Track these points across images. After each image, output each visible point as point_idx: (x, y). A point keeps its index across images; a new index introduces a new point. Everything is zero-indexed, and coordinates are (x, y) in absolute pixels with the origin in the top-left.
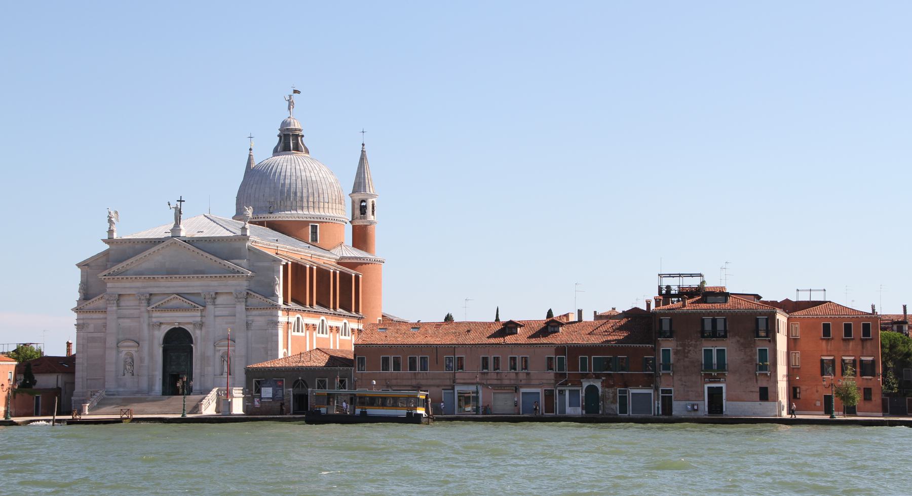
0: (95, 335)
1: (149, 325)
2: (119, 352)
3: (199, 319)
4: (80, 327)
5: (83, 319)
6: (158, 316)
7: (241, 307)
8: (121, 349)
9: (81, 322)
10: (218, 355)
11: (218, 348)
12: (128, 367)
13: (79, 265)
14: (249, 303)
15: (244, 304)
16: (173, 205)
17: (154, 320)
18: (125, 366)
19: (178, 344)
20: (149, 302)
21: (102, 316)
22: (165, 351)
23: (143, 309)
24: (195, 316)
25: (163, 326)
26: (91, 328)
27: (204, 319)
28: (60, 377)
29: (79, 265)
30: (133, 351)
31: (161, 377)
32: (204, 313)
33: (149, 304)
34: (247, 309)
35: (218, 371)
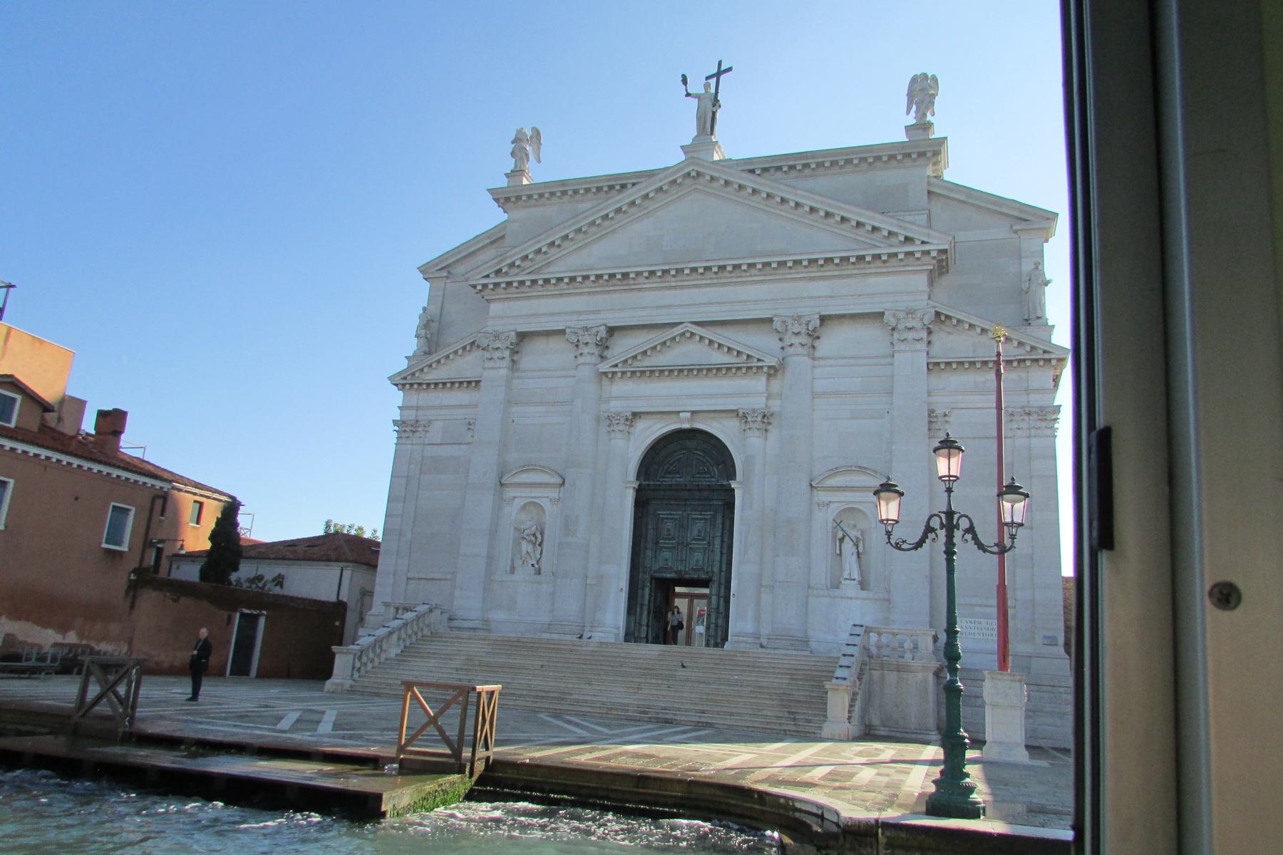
0: (444, 451)
1: (598, 420)
2: (500, 502)
3: (759, 403)
4: (406, 428)
5: (418, 408)
6: (628, 394)
7: (912, 359)
8: (510, 492)
9: (411, 415)
10: (823, 520)
11: (822, 496)
12: (526, 547)
13: (424, 270)
14: (937, 349)
15: (922, 346)
16: (696, 86)
17: (616, 406)
18: (517, 543)
19: (685, 482)
20: (603, 346)
21: (463, 397)
22: (642, 503)
23: (586, 372)
24: (750, 392)
25: (641, 425)
26: (435, 433)
27: (775, 405)
28: (347, 573)
29: (424, 270)
30: (545, 497)
31: (623, 583)
32: (776, 384)
33: (602, 357)
34: (933, 367)
35: (820, 574)
